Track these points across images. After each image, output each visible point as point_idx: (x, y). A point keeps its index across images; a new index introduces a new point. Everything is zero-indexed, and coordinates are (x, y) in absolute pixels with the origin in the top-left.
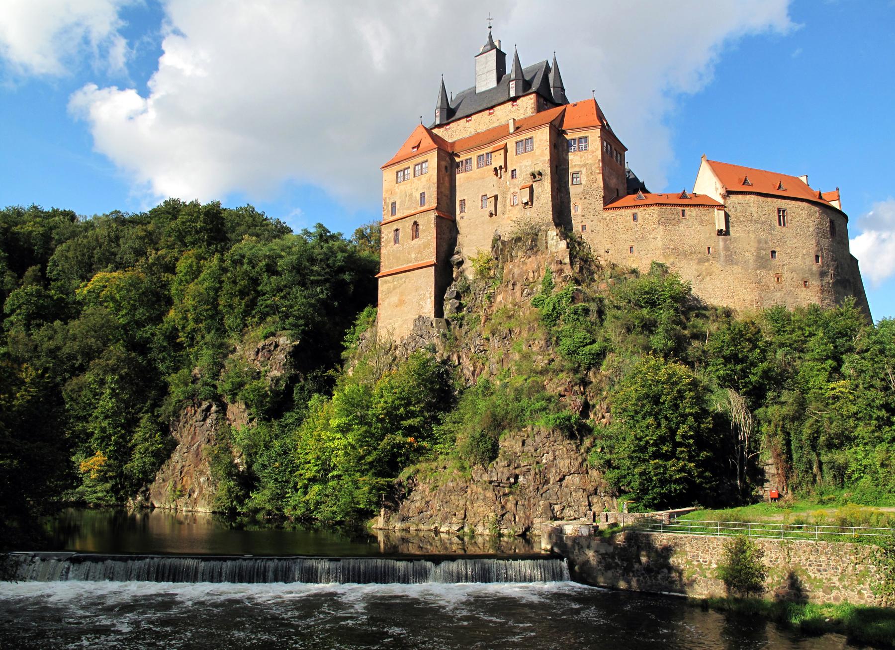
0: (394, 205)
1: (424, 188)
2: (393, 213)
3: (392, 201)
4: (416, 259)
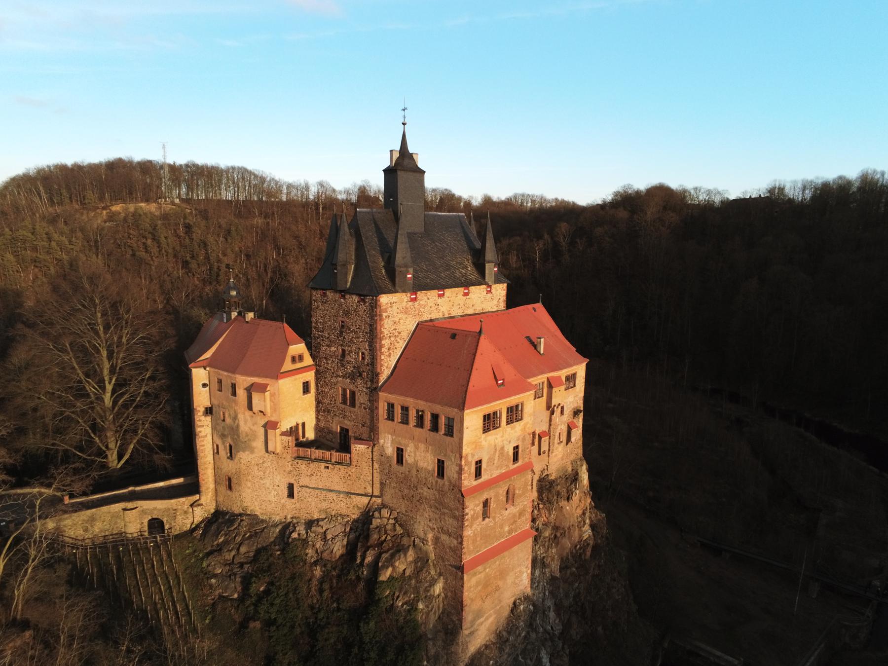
0: (479, 463)
1: (518, 440)
2: (478, 473)
3: (477, 458)
4: (510, 532)
